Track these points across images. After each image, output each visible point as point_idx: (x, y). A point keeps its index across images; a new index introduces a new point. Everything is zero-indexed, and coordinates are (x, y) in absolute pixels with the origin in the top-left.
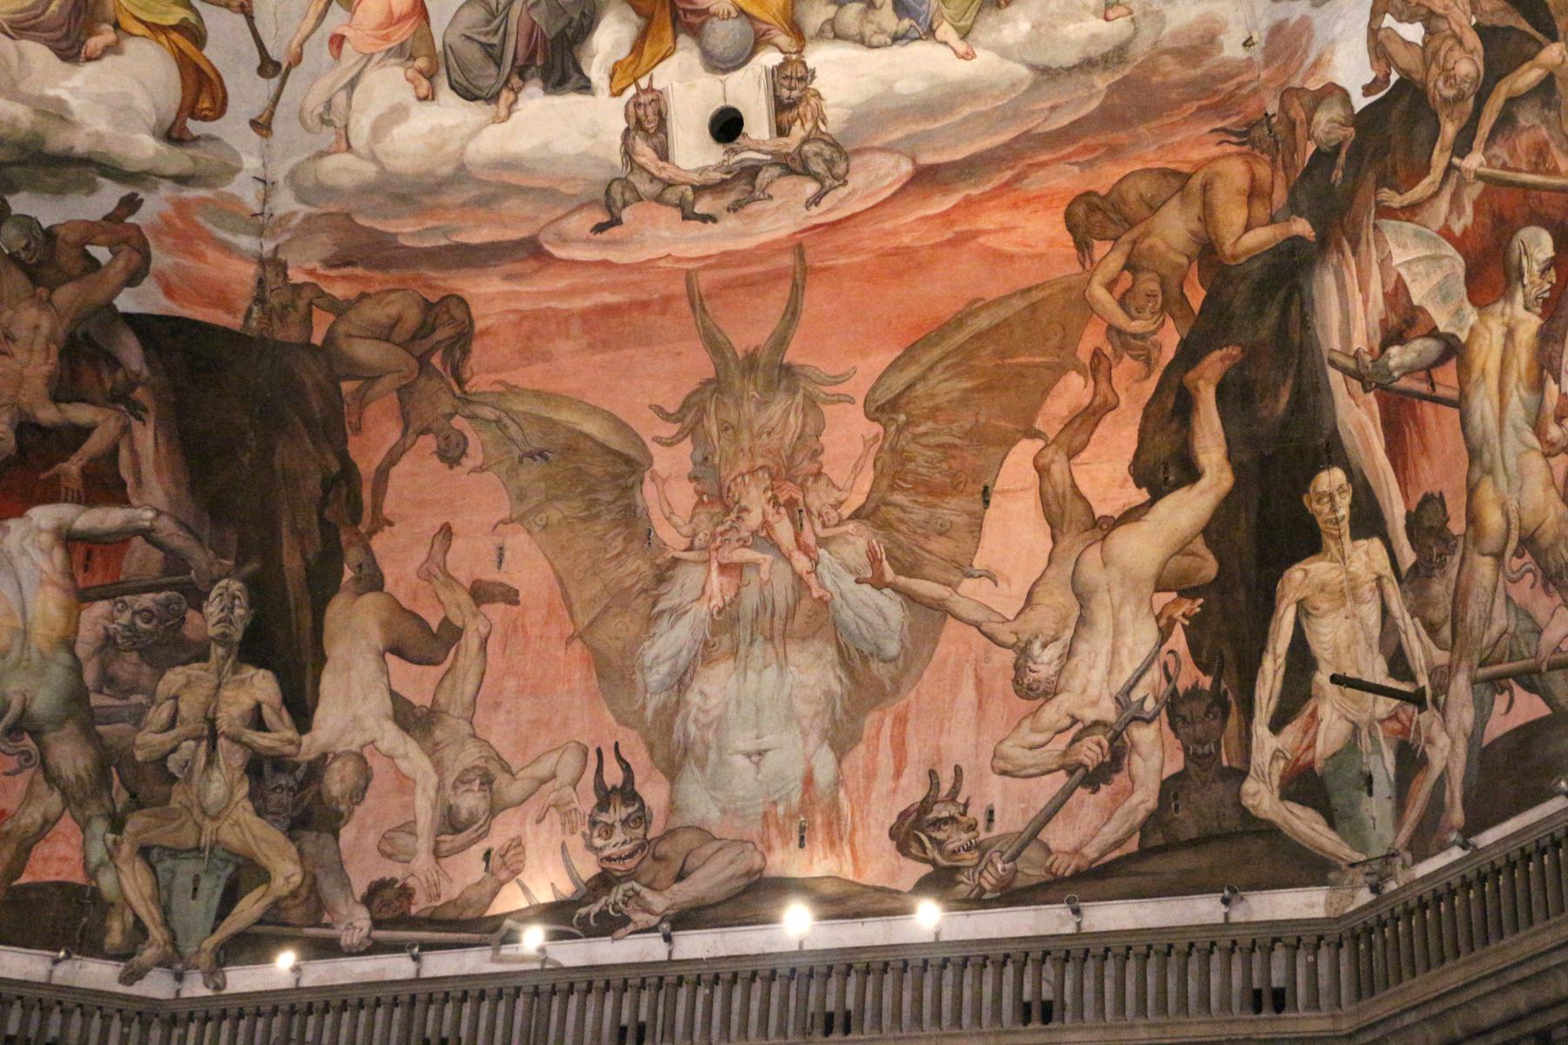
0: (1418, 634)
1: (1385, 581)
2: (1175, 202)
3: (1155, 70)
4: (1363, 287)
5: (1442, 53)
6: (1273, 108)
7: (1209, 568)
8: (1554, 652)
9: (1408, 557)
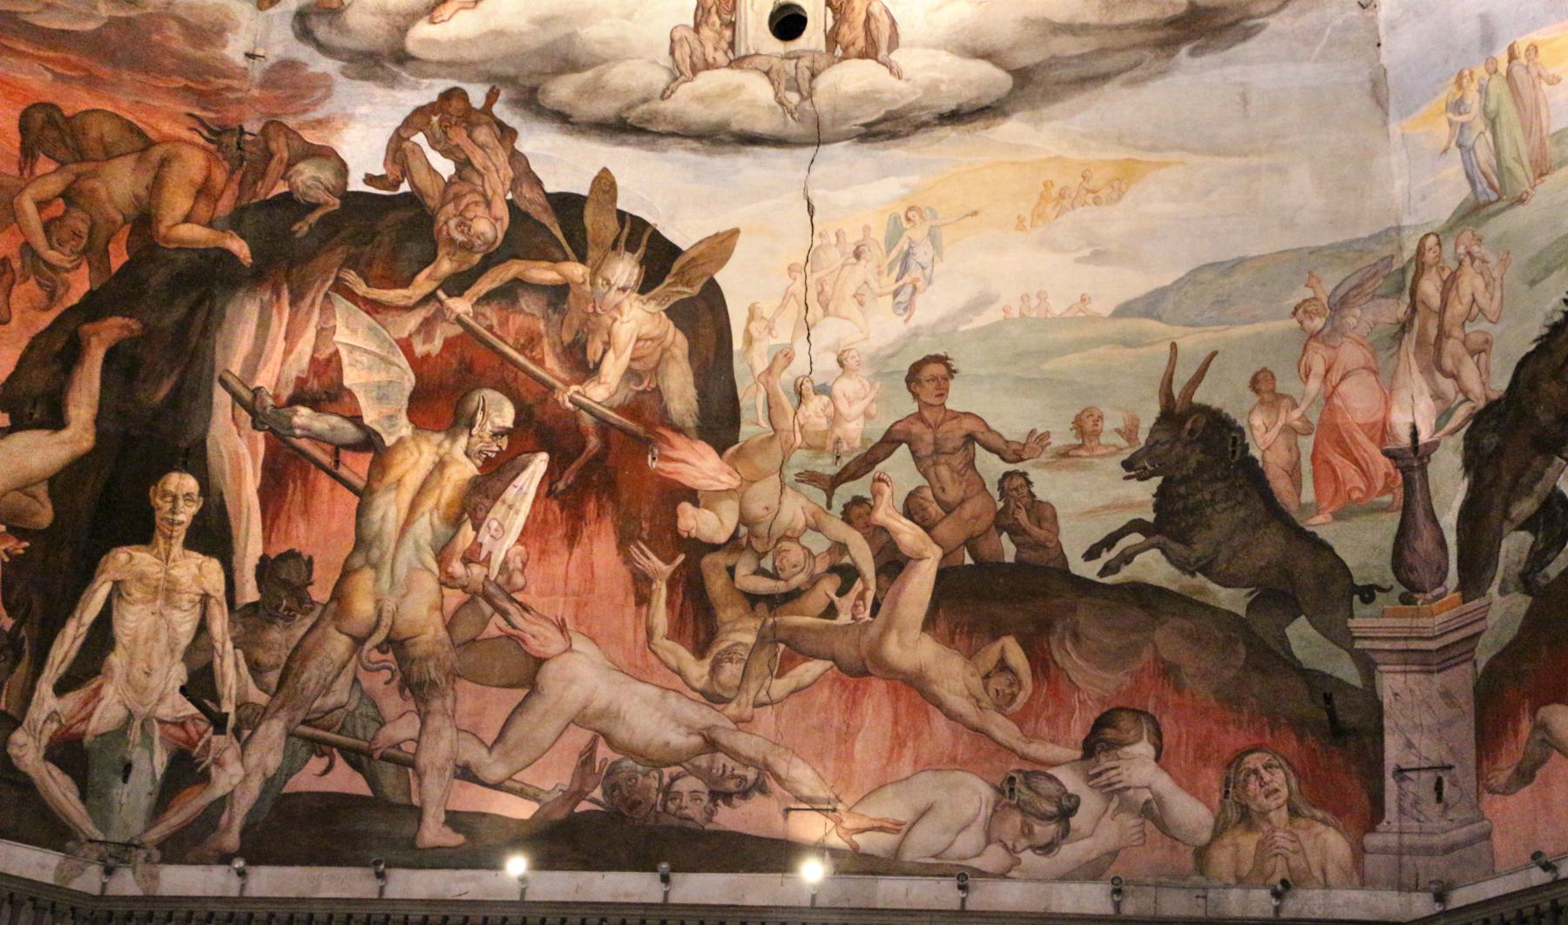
0: (237, 666)
1: (212, 601)
2: (130, 161)
3: (159, 30)
4: (291, 337)
5: (464, 202)
6: (253, 126)
7: (45, 516)
8: (393, 747)
9: (249, 592)
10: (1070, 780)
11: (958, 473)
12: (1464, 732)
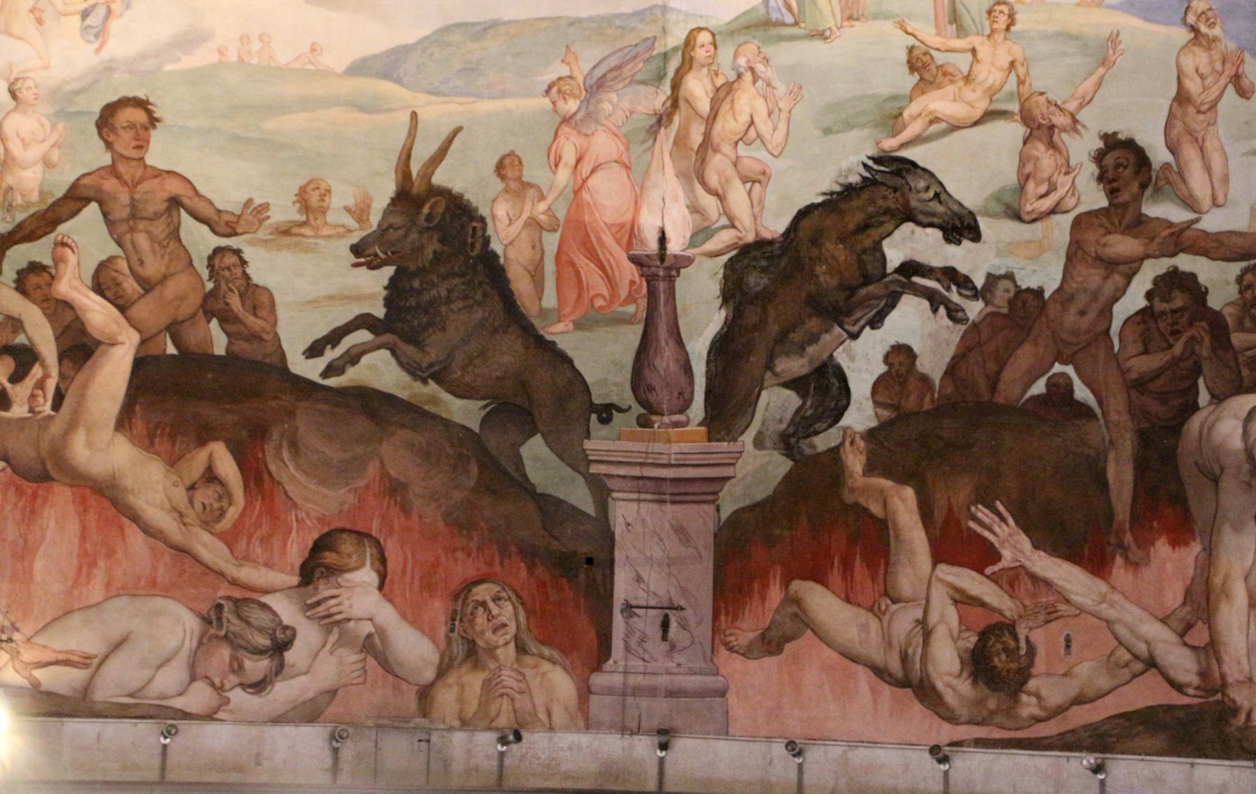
10: (285, 609)
11: (160, 244)
12: (701, 578)
